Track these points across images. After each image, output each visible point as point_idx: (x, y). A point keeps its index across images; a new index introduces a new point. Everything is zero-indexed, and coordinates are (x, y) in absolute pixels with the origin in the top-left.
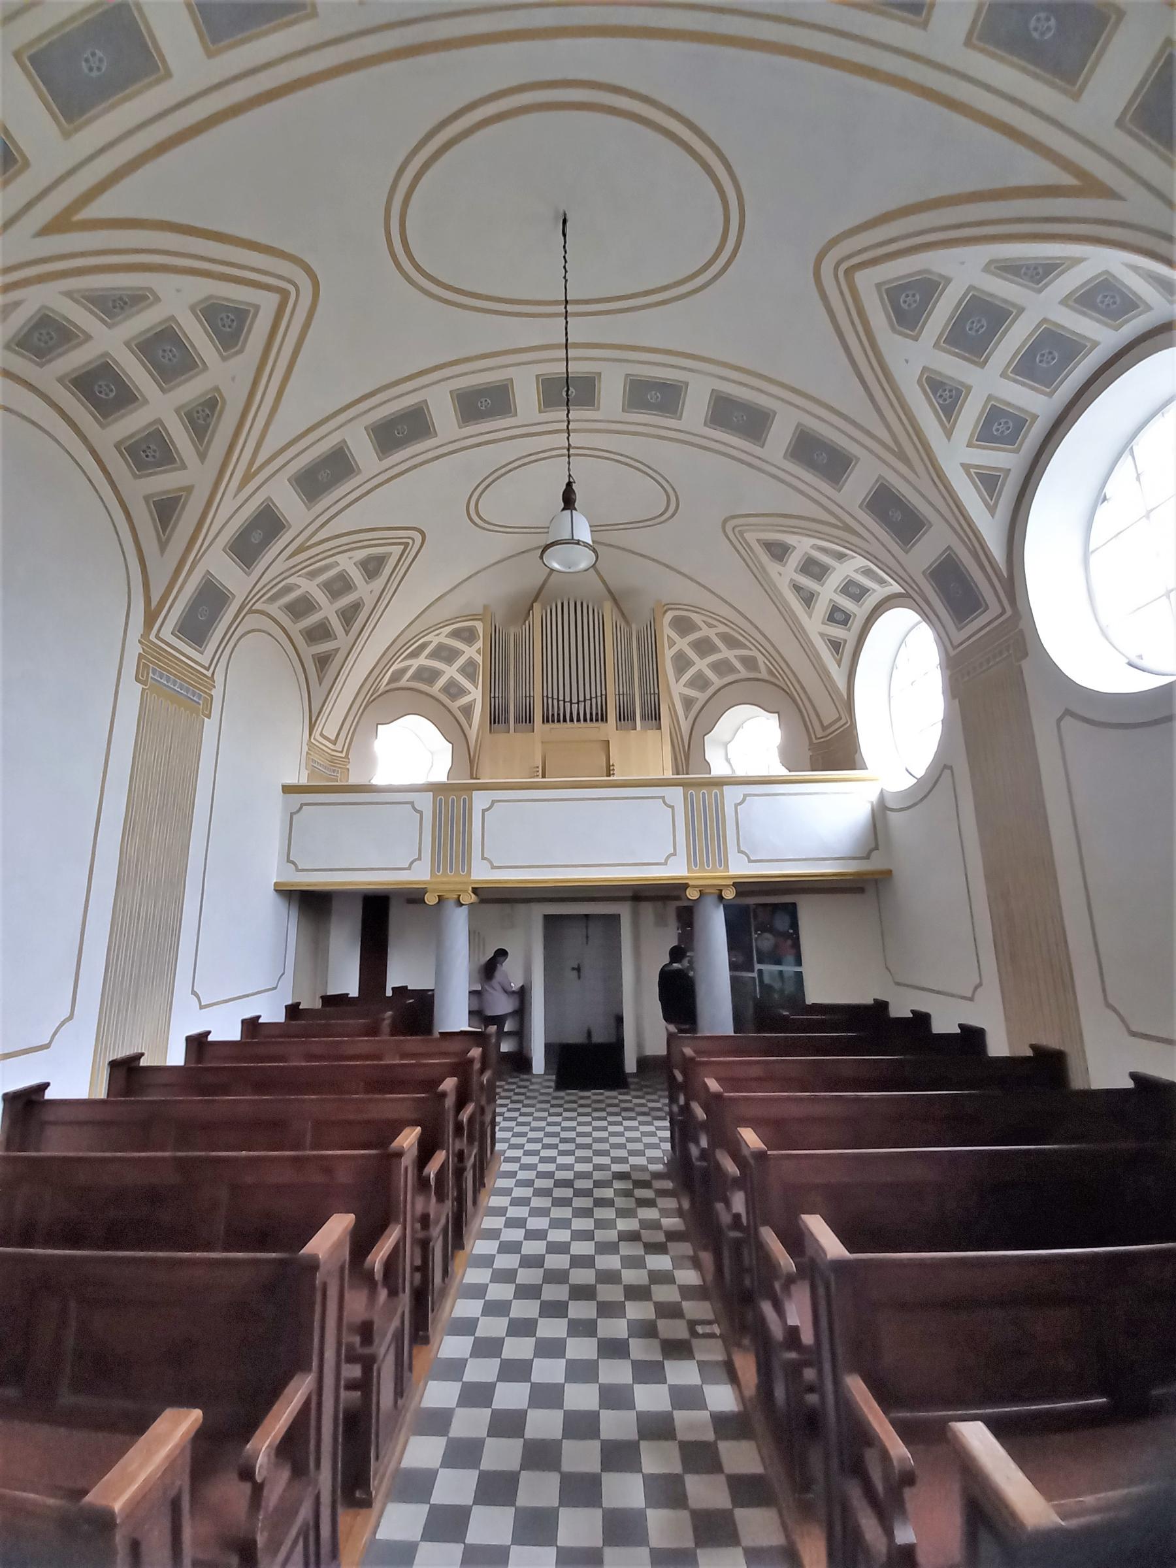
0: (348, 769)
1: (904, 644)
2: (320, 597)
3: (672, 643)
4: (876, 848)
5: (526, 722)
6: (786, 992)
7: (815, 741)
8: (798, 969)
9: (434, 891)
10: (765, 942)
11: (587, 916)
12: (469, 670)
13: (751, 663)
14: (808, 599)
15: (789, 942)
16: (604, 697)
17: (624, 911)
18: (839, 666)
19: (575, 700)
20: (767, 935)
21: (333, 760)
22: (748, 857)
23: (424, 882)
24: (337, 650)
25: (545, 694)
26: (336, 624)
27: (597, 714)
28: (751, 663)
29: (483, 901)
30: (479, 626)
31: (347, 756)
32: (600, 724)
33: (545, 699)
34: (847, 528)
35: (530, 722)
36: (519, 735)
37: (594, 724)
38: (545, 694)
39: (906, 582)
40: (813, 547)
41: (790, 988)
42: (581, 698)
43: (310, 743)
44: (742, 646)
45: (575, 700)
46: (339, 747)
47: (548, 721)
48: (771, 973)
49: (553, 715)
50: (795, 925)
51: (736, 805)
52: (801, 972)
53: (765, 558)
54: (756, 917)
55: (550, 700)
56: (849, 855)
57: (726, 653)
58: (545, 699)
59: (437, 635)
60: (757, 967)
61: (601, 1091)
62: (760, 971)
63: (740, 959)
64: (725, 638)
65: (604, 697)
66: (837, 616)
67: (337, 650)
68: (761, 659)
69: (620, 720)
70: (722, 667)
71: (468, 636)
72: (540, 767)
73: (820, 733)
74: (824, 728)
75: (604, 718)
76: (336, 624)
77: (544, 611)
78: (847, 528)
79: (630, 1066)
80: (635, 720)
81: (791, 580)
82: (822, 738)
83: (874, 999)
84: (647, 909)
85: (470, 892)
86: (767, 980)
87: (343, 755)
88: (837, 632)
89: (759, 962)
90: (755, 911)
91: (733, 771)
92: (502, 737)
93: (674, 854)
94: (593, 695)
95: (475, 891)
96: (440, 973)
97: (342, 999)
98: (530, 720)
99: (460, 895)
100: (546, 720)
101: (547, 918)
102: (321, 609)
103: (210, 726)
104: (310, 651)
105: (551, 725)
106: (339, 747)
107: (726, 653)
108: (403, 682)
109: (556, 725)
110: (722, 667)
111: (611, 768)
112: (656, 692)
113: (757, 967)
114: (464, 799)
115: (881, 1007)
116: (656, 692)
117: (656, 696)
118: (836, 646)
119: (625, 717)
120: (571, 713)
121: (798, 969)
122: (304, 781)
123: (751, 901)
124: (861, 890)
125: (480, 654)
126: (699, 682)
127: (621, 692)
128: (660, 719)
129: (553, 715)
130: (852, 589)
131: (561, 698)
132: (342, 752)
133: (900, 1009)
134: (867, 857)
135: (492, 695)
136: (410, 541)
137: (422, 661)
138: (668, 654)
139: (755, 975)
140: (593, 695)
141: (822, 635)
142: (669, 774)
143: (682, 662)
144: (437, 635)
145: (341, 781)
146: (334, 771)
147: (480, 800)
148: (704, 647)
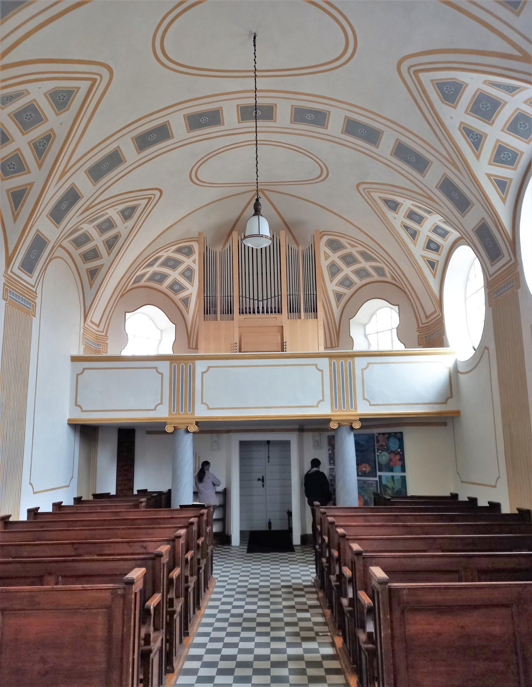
0: (107, 344)
1: (473, 265)
2: (94, 233)
3: (327, 257)
4: (451, 397)
5: (228, 313)
6: (396, 490)
7: (421, 326)
8: (403, 474)
9: (171, 423)
10: (383, 457)
11: (268, 442)
12: (188, 274)
13: (380, 271)
14: (414, 235)
15: (398, 457)
16: (280, 297)
17: (293, 438)
18: (434, 277)
19: (260, 299)
20: (385, 453)
21: (97, 337)
22: (369, 402)
23: (166, 419)
24: (102, 266)
25: (241, 295)
26: (103, 250)
27: (275, 308)
28: (380, 271)
29: (201, 432)
30: (196, 246)
31: (106, 335)
32: (277, 315)
33: (241, 297)
34: (430, 198)
35: (231, 313)
36: (223, 322)
37: (274, 315)
38: (241, 295)
39: (464, 233)
40: (412, 205)
41: (398, 486)
42: (265, 298)
43: (85, 328)
44: (375, 260)
45: (260, 299)
46: (101, 328)
47: (243, 313)
48: (387, 477)
49: (246, 308)
50: (401, 446)
51: (363, 370)
52: (405, 477)
53: (385, 209)
54: (378, 442)
55: (244, 298)
56: (435, 402)
57: (364, 264)
58: (241, 297)
59: (167, 251)
60: (379, 473)
61: (278, 553)
62: (380, 477)
63: (366, 468)
64: (363, 254)
65: (280, 297)
66: (432, 246)
67: (102, 266)
68: (386, 269)
69: (290, 312)
70: (361, 273)
71: (189, 252)
72: (238, 344)
73: (424, 320)
74: (427, 317)
75: (280, 311)
76: (103, 250)
77: (240, 237)
78: (430, 198)
79: (296, 540)
80: (299, 311)
81: (402, 222)
82: (425, 323)
83: (451, 493)
84: (308, 437)
85: (194, 424)
86: (384, 482)
87: (104, 334)
88: (432, 256)
89: (380, 471)
90: (377, 437)
91: (370, 345)
92: (212, 323)
93: (323, 400)
94: (273, 295)
95: (197, 423)
96: (175, 477)
97: (107, 496)
98: (230, 311)
99: (188, 426)
100: (241, 312)
101: (243, 444)
102: (94, 240)
103: (36, 321)
104: (85, 267)
105: (244, 316)
106: (101, 328)
107: (364, 264)
108: (142, 283)
109: (248, 316)
110: (361, 273)
111: (284, 344)
112: (315, 293)
113: (379, 473)
114: (190, 366)
115: (455, 496)
116: (315, 293)
117: (315, 296)
118: (432, 264)
119: (294, 310)
120: (258, 308)
121: (403, 474)
122: (82, 353)
123: (376, 431)
124: (445, 424)
125: (195, 263)
126: (346, 282)
127: (291, 294)
128: (317, 311)
129: (246, 308)
130: (439, 231)
131: (251, 297)
132: (103, 332)
133: (463, 498)
134: (445, 403)
135: (206, 295)
136: (153, 196)
137: (156, 268)
138: (323, 264)
139: (377, 479)
140: (273, 295)
141: (423, 257)
142: (322, 350)
143: (334, 270)
144: (167, 251)
145: (103, 352)
146: (98, 345)
147: (200, 366)
148: (349, 260)
